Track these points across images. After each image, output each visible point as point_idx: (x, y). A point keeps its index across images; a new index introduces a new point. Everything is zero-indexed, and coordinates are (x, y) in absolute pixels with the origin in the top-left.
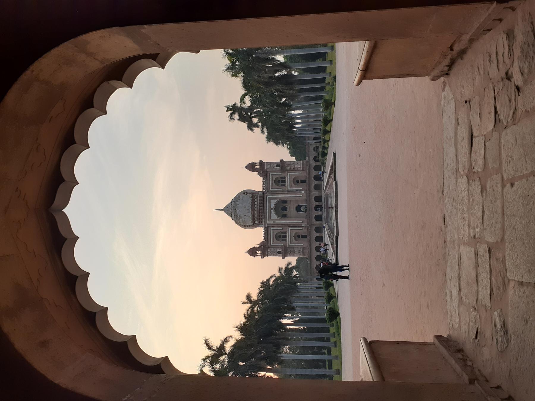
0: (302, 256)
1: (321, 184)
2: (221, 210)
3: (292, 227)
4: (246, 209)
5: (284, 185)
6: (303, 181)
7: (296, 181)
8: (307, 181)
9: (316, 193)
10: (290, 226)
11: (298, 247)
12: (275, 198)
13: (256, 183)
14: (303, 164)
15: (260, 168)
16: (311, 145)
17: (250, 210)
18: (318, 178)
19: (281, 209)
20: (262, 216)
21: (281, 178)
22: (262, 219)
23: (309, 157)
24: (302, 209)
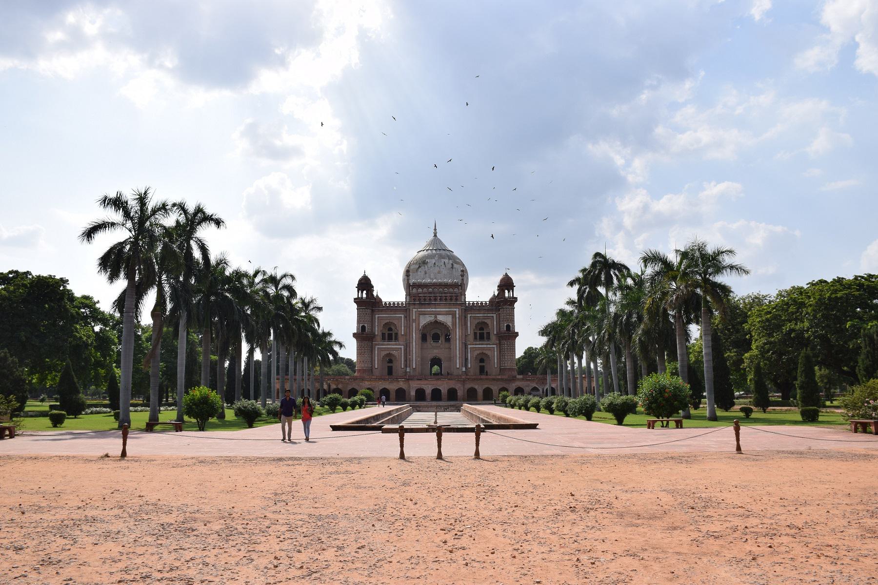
3: (405, 350)
5: (475, 338)
6: (482, 370)
7: (482, 359)
8: (483, 377)
10: (407, 346)
11: (372, 361)
12: (454, 324)
13: (480, 290)
18: (488, 397)
19: (436, 333)
20: (425, 300)
21: (488, 334)
22: (419, 300)
24: (436, 368)
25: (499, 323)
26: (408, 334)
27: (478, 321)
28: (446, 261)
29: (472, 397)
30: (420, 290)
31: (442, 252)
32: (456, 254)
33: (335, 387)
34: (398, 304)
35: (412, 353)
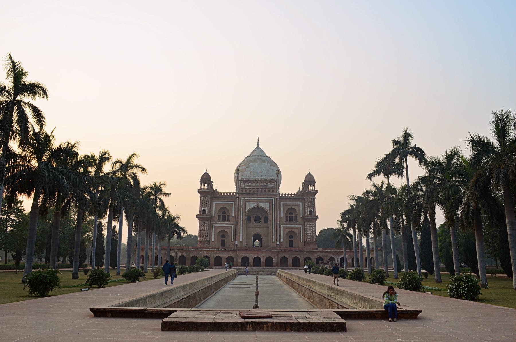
1: (288, 266)
2: (258, 145)
4: (258, 176)
5: (287, 220)
6: (291, 244)
7: (291, 235)
10: (236, 225)
11: (210, 236)
13: (290, 185)
15: (308, 191)
17: (257, 177)
18: (296, 263)
19: (257, 216)
20: (250, 191)
21: (296, 217)
22: (246, 191)
23: (322, 252)
27: (289, 207)
28: (266, 164)
29: (284, 263)
30: (246, 184)
32: (272, 159)
33: (181, 255)
34: (230, 194)
35: (240, 232)
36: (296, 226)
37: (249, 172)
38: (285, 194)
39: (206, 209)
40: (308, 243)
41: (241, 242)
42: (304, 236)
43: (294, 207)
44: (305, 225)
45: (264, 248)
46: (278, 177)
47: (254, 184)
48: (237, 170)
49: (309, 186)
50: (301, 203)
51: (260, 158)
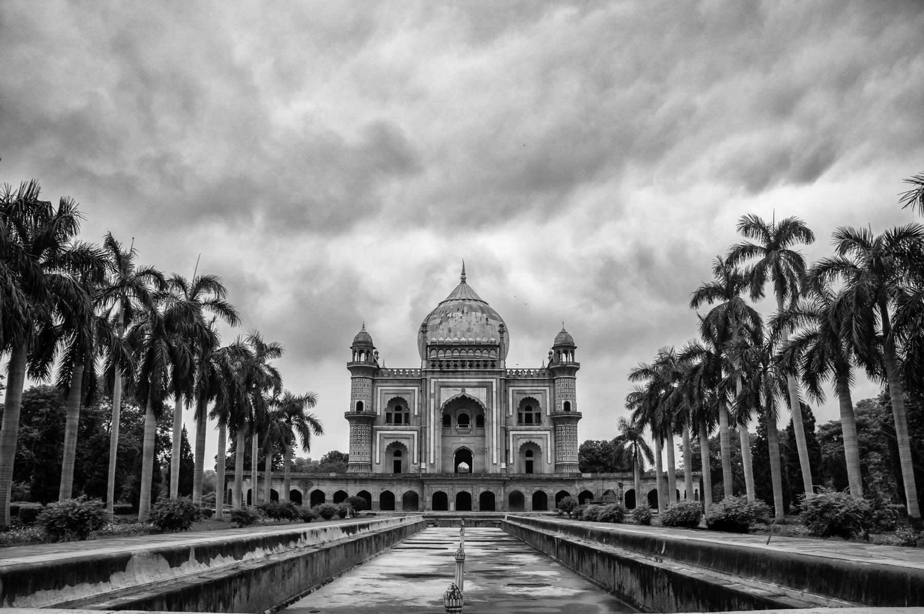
0: (352, 460)
5: (520, 422)
6: (529, 467)
9: (501, 497)
10: (422, 433)
13: (526, 355)
14: (570, 466)
16: (621, 485)
17: (463, 339)
18: (540, 502)
19: (463, 414)
20: (448, 366)
21: (539, 415)
22: (440, 366)
24: (464, 465)
25: (553, 400)
26: (423, 416)
27: (524, 397)
28: (479, 314)
30: (441, 355)
31: (472, 303)
32: (491, 306)
36: (539, 433)
37: (446, 331)
38: (517, 372)
39: (363, 401)
40: (562, 466)
41: (432, 465)
42: (555, 452)
43: (535, 397)
44: (555, 429)
45: (477, 474)
46: (502, 338)
47: (456, 354)
48: (424, 326)
49: (564, 355)
50: (547, 389)
51: (467, 303)
